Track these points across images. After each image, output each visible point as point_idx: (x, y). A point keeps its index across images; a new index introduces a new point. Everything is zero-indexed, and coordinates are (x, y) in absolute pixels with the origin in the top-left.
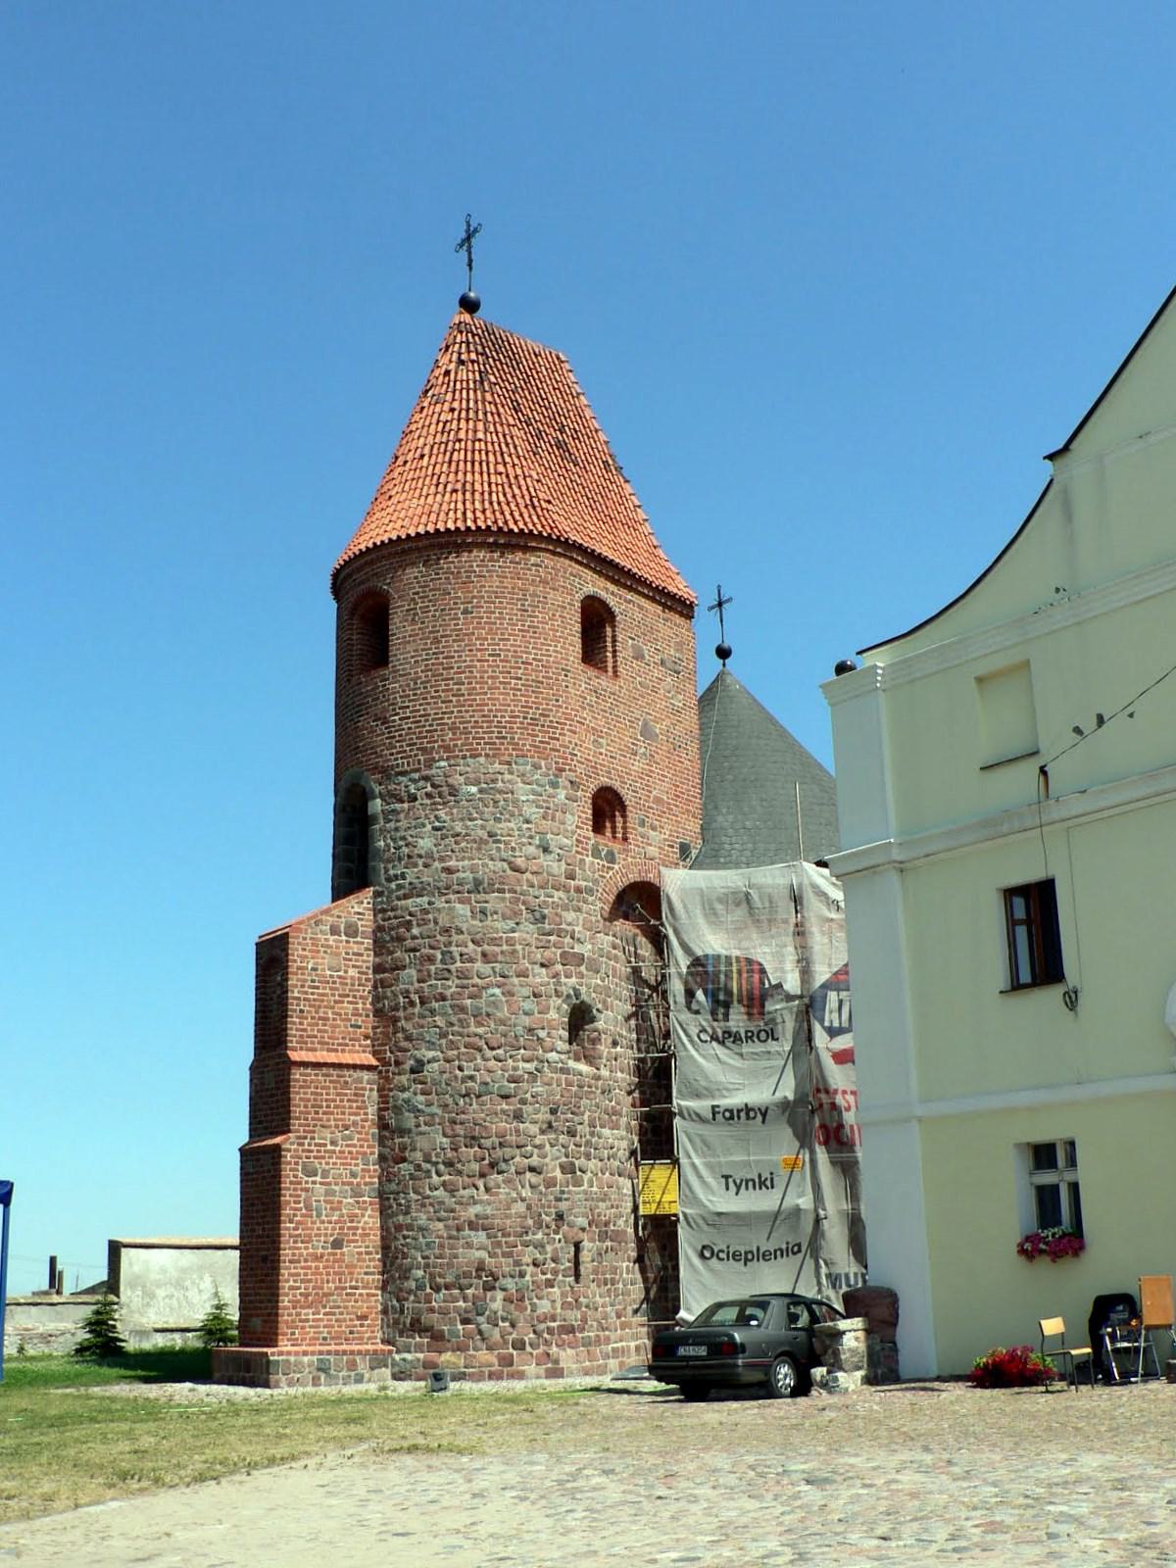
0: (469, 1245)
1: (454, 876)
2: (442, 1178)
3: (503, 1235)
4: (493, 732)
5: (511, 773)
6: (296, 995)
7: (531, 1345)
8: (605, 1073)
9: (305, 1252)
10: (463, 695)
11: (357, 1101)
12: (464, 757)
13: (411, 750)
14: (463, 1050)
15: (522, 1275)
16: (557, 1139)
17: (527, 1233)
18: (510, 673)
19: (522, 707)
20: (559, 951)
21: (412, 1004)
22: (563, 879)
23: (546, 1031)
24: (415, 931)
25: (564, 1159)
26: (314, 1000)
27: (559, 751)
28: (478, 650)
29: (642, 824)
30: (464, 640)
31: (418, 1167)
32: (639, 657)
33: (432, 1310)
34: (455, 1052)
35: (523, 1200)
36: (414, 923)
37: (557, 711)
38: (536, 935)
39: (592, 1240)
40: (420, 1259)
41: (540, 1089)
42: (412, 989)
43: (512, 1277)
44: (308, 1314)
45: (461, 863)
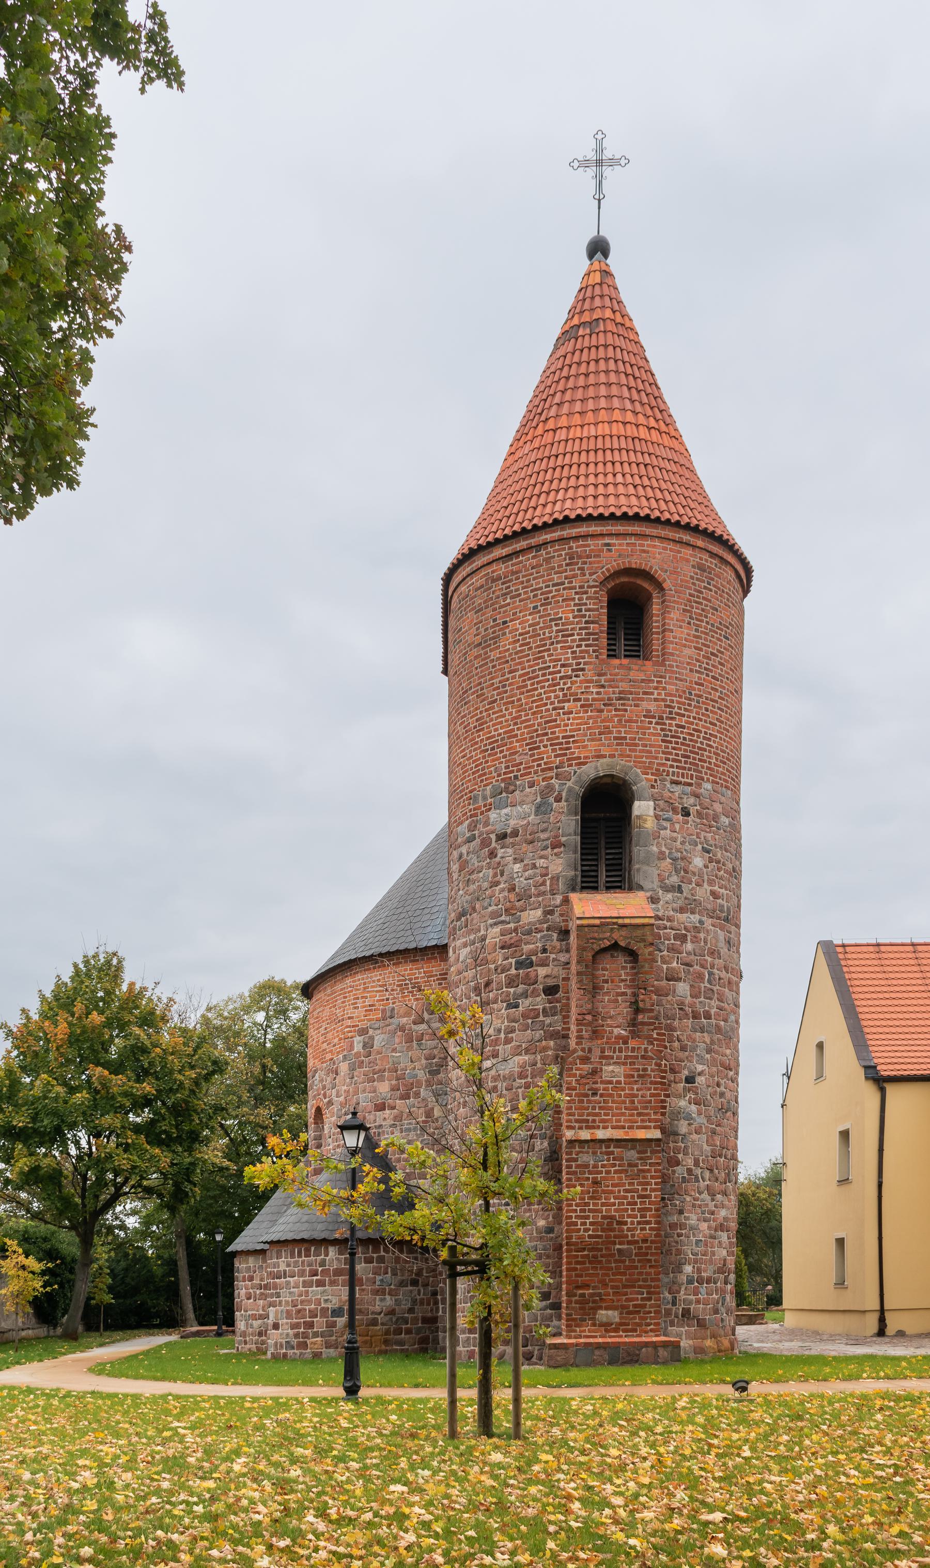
13: (686, 762)
24: (689, 946)
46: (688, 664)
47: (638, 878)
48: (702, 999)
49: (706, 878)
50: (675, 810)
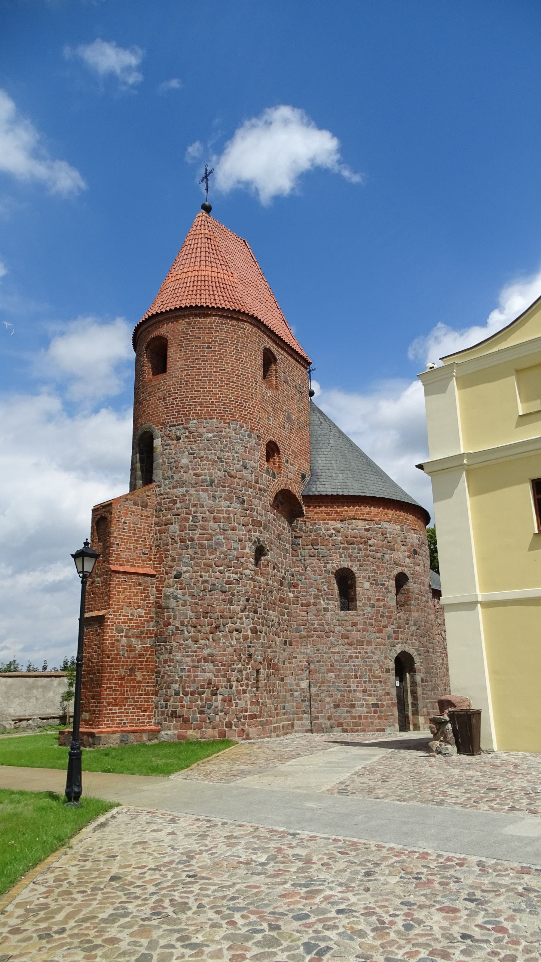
0: (204, 671)
1: (200, 478)
2: (190, 634)
3: (222, 666)
4: (221, 408)
5: (229, 428)
6: (115, 535)
7: (235, 725)
8: (270, 582)
9: (115, 675)
10: (206, 388)
11: (145, 593)
12: (206, 419)
13: (178, 415)
14: (203, 567)
15: (231, 686)
16: (249, 615)
17: (234, 664)
18: (229, 379)
19: (235, 396)
20: (251, 519)
21: (176, 542)
22: (253, 483)
23: (244, 559)
24: (178, 505)
25: (252, 626)
26: (125, 539)
27: (252, 420)
28: (214, 367)
29: (287, 461)
30: (207, 361)
31: (177, 628)
32: (286, 382)
33: (183, 706)
34: (198, 568)
35: (232, 646)
36: (178, 501)
37: (252, 401)
38: (240, 510)
39: (264, 669)
40: (177, 678)
41: (241, 588)
42: (176, 534)
43: (226, 688)
44: (115, 709)
45: (203, 472)
46: (180, 368)
47: (154, 477)
48: (187, 531)
49: (190, 467)
50: (172, 439)
